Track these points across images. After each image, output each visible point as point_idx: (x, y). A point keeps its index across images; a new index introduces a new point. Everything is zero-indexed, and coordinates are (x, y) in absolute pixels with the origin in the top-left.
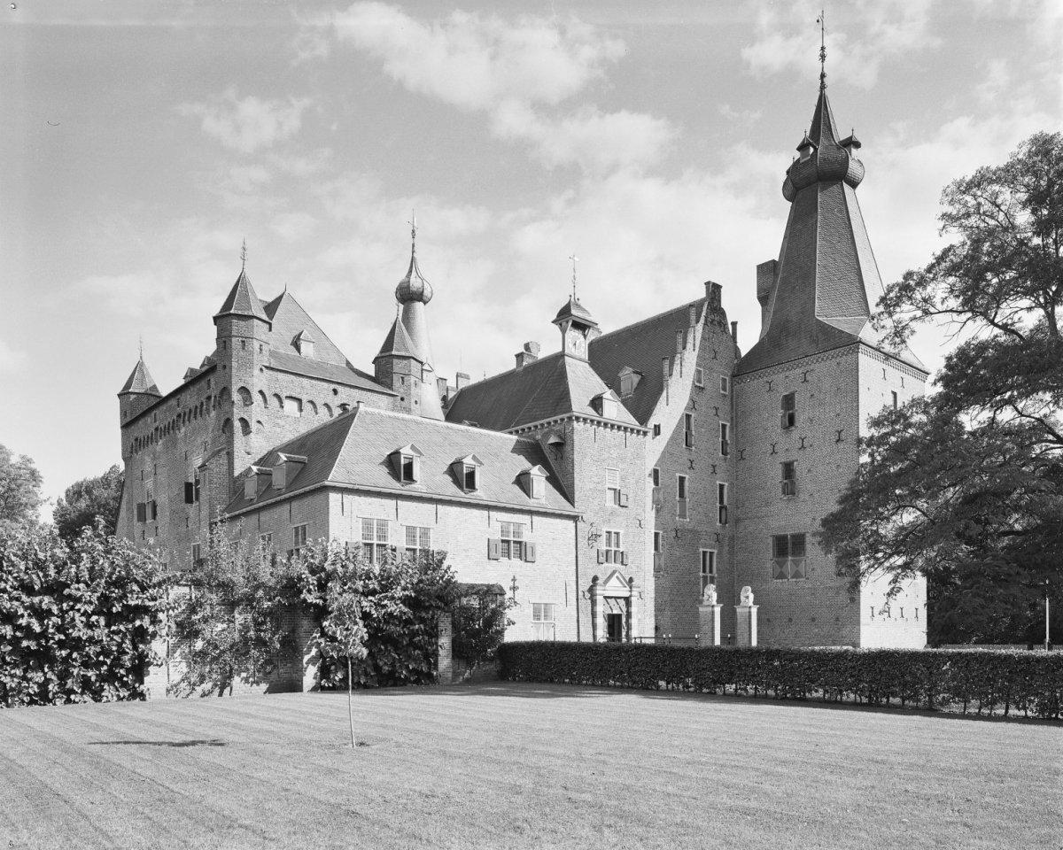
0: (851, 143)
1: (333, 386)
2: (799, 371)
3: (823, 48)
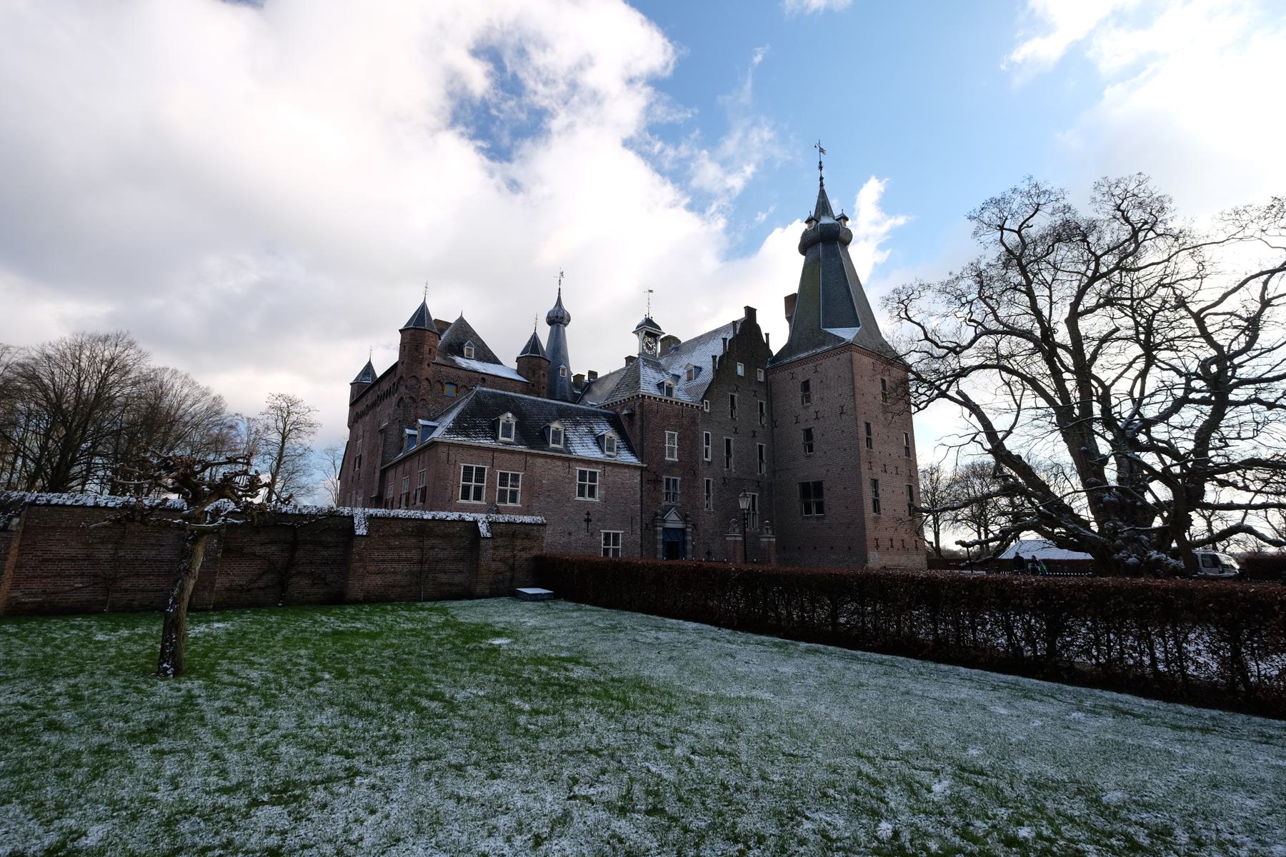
2: (811, 365)
3: (820, 163)
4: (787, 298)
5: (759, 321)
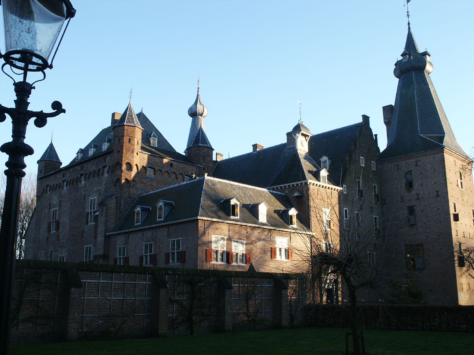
0: (425, 54)
2: (414, 160)
4: (384, 108)
5: (371, 126)
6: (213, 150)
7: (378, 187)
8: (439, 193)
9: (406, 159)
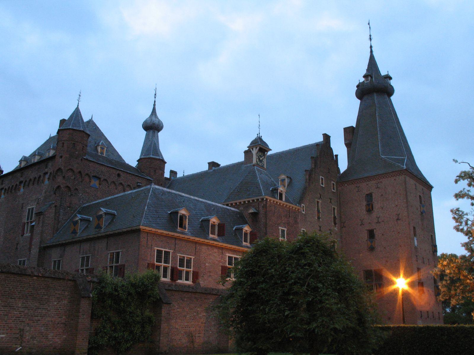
1: (118, 172)
2: (375, 182)
3: (370, 36)
4: (344, 128)
5: (332, 146)
6: (166, 163)
7: (337, 209)
8: (400, 216)
9: (366, 181)
